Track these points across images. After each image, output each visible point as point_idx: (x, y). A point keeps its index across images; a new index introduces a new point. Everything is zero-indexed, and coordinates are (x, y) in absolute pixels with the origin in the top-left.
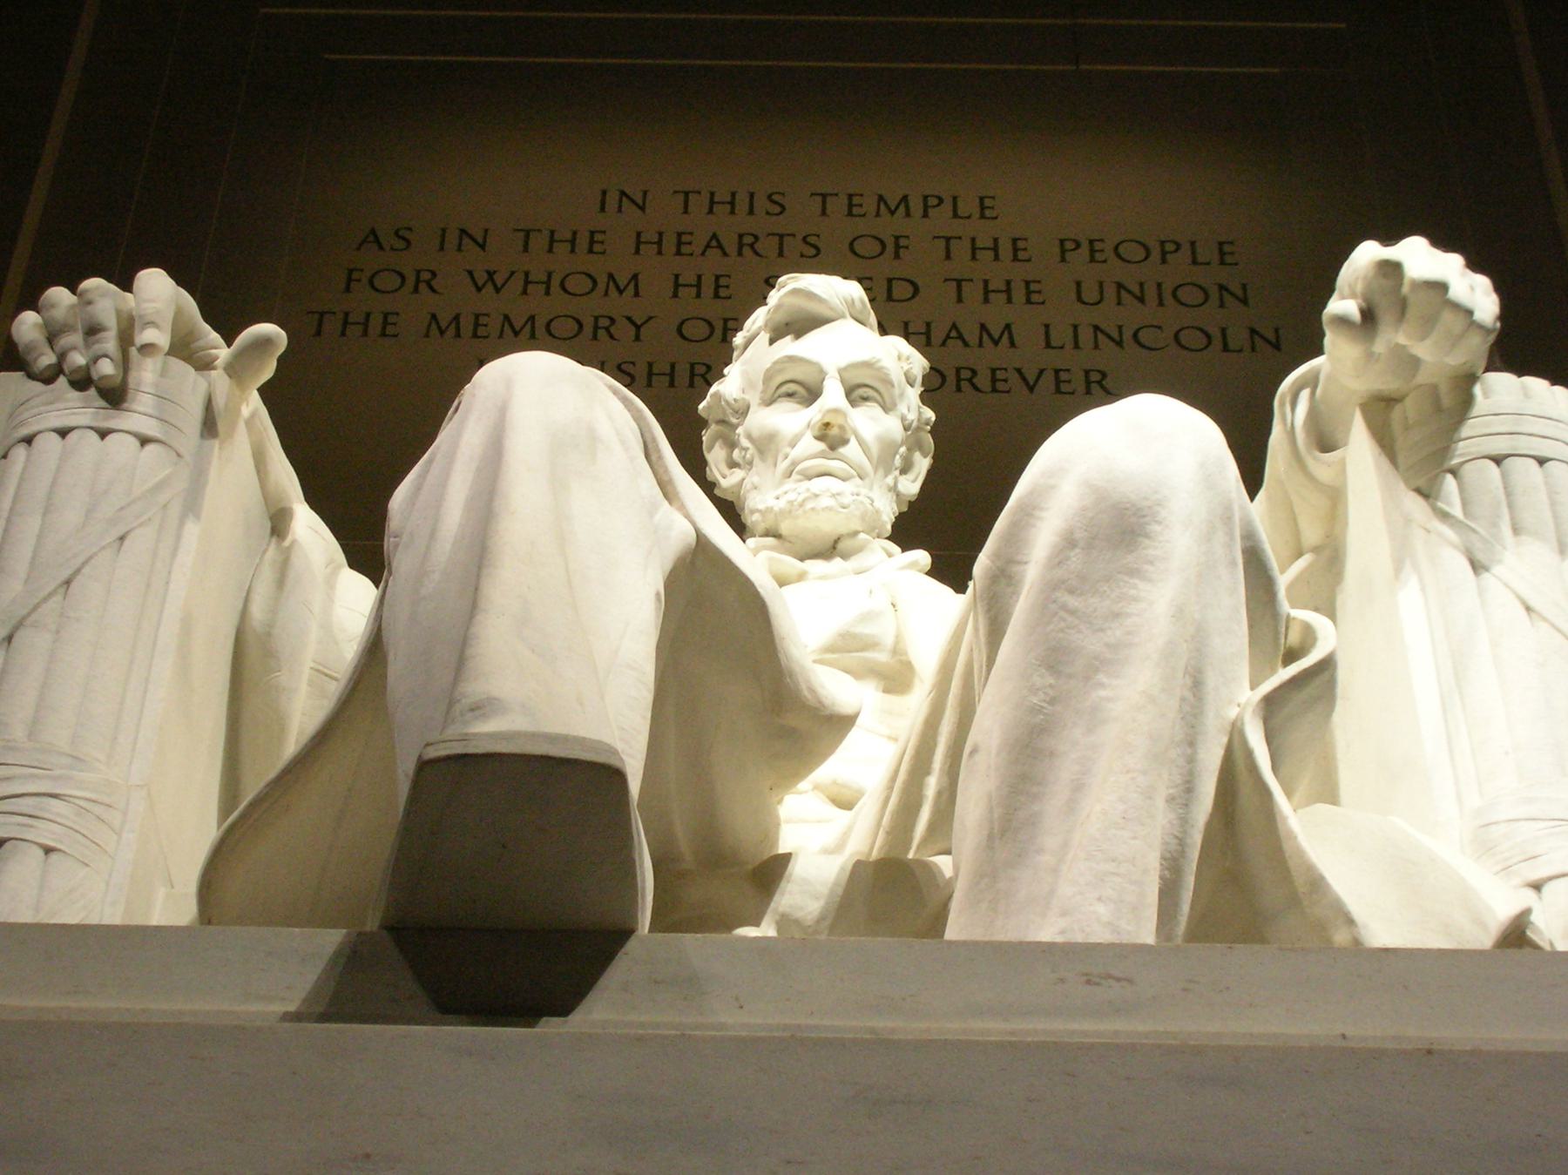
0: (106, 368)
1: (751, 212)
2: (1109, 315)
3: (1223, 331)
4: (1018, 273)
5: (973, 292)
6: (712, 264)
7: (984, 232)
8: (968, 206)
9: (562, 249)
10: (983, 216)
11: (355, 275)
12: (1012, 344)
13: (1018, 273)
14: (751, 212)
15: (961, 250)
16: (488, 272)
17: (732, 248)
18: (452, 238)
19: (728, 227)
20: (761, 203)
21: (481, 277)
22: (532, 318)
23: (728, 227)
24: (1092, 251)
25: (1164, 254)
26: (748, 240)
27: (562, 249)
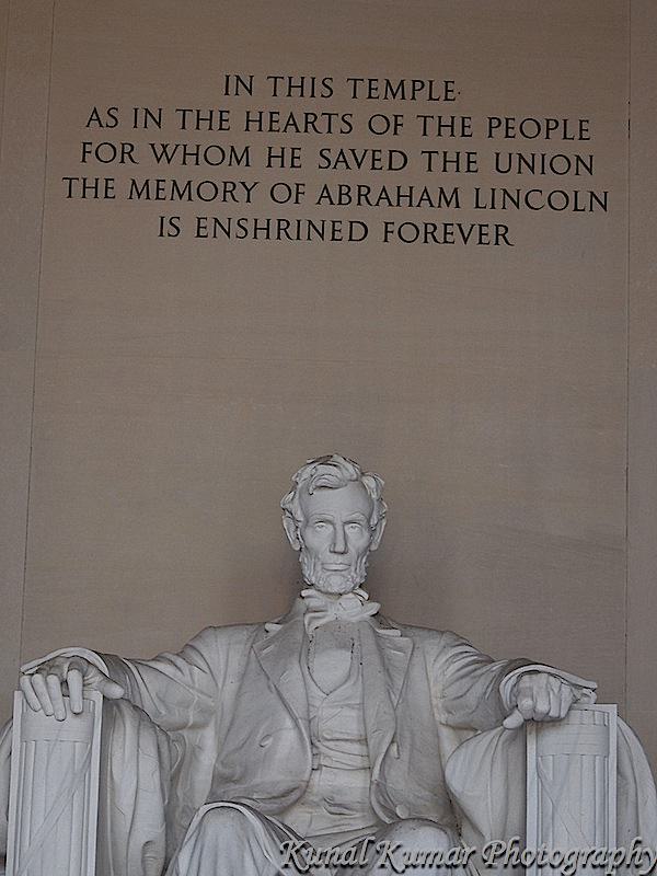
0: (61, 718)
1: (313, 96)
2: (513, 182)
3: (576, 192)
4: (464, 146)
5: (437, 160)
6: (290, 139)
7: (445, 110)
8: (439, 91)
9: (204, 125)
10: (446, 99)
11: (88, 148)
12: (458, 206)
13: (464, 146)
14: (313, 96)
15: (432, 125)
16: (163, 145)
17: (302, 128)
18: (141, 114)
19: (300, 106)
20: (319, 86)
21: (159, 150)
22: (189, 183)
23: (300, 106)
24: (507, 128)
25: (548, 129)
26: (311, 118)
27: (204, 125)
